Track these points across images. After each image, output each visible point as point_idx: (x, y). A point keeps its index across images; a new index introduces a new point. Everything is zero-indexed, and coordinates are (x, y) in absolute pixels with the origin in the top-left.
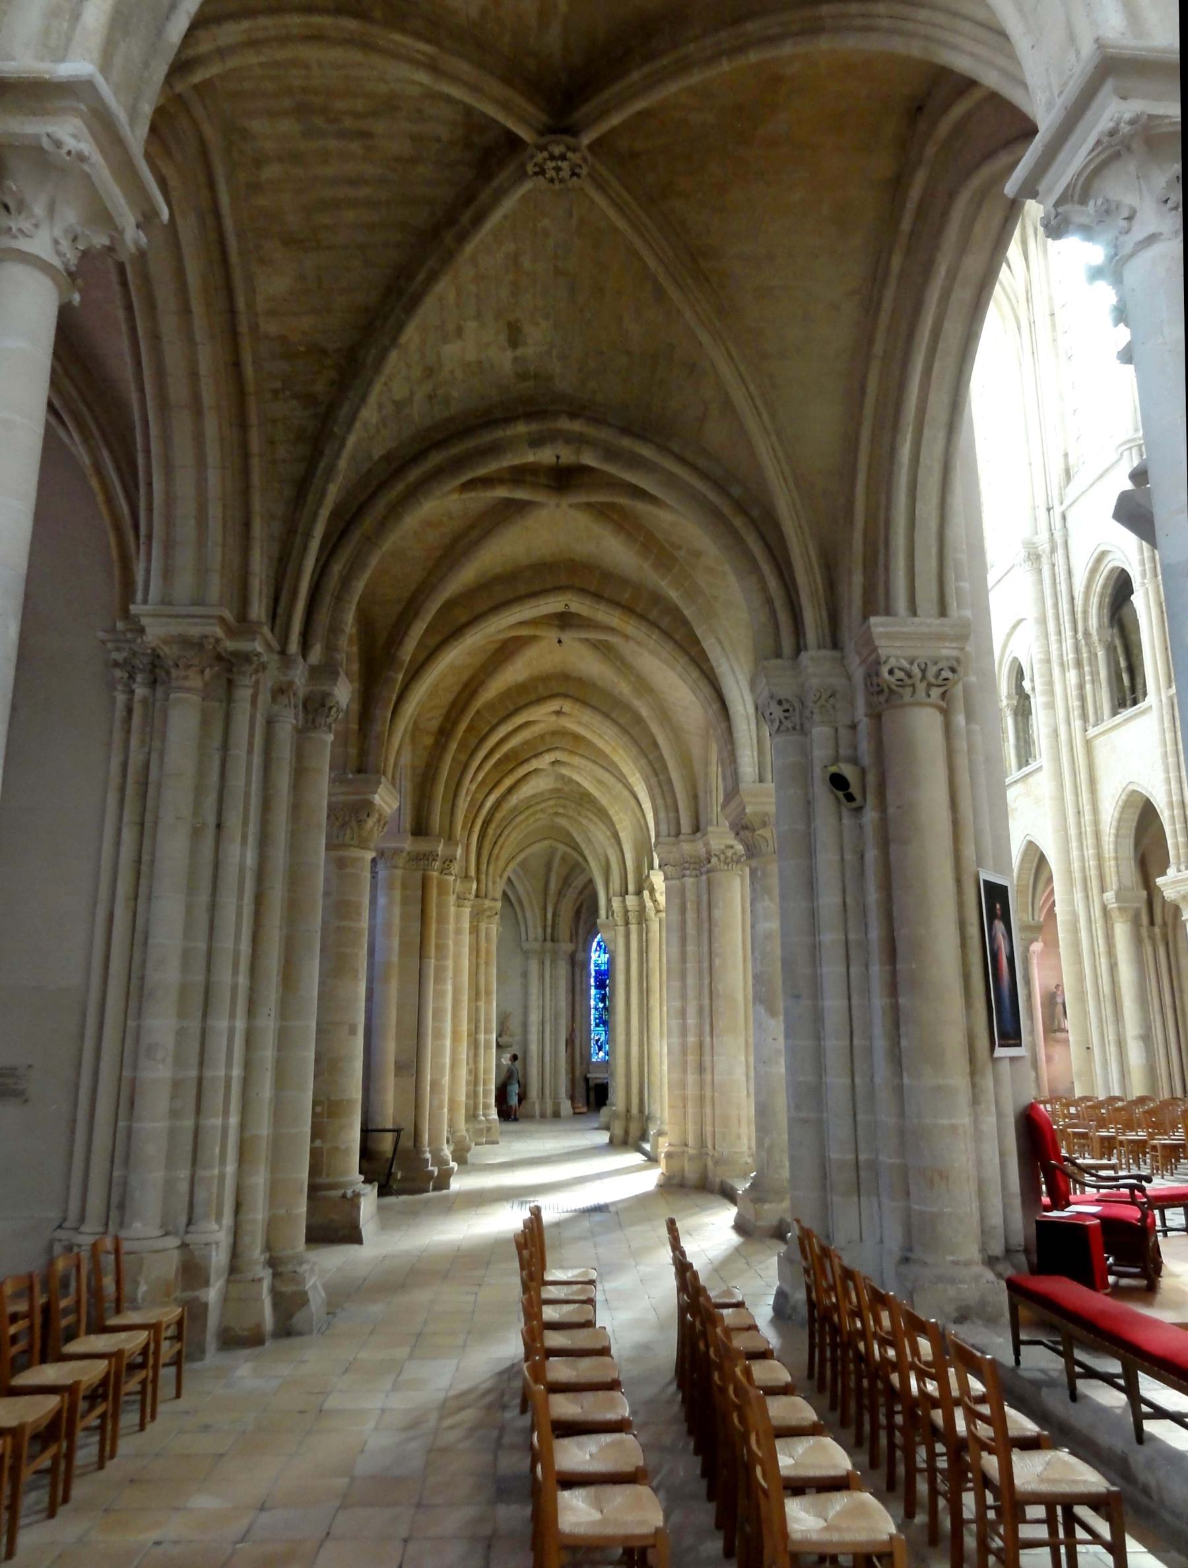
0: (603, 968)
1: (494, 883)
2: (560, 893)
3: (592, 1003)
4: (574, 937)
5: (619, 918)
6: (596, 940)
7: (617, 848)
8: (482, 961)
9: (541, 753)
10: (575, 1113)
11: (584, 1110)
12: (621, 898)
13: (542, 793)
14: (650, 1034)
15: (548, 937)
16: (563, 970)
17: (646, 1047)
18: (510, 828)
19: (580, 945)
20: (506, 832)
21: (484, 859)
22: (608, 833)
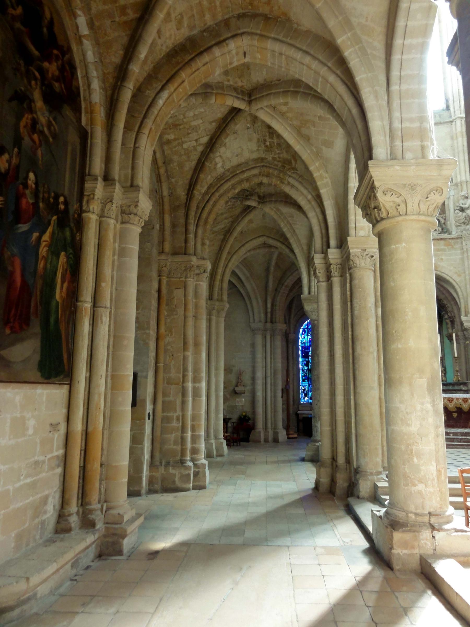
0: (306, 345)
1: (203, 244)
2: (276, 290)
3: (300, 366)
4: (287, 321)
5: (321, 274)
6: (302, 328)
7: (318, 210)
8: (190, 313)
9: (224, 40)
10: (288, 438)
11: (296, 436)
12: (323, 255)
13: (246, 163)
14: (358, 383)
15: (269, 320)
16: (279, 343)
17: (352, 397)
18: (217, 194)
19: (292, 326)
20: (214, 199)
21: (192, 221)
22: (310, 197)
